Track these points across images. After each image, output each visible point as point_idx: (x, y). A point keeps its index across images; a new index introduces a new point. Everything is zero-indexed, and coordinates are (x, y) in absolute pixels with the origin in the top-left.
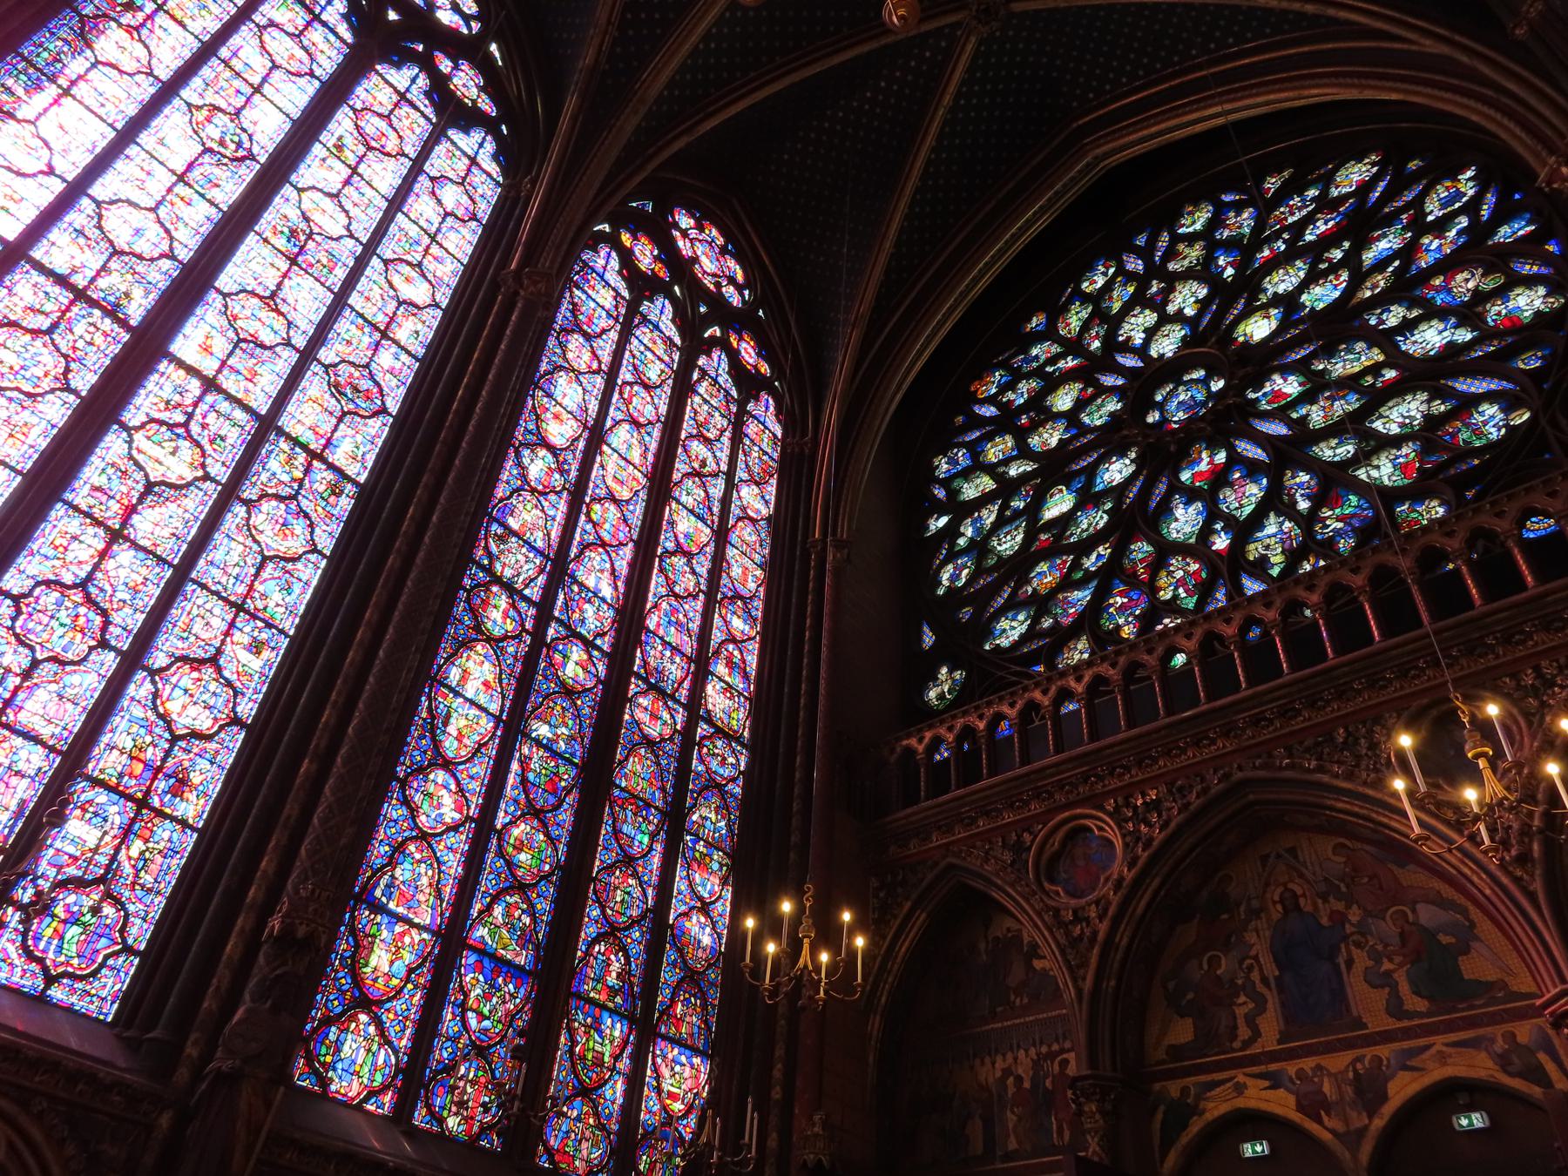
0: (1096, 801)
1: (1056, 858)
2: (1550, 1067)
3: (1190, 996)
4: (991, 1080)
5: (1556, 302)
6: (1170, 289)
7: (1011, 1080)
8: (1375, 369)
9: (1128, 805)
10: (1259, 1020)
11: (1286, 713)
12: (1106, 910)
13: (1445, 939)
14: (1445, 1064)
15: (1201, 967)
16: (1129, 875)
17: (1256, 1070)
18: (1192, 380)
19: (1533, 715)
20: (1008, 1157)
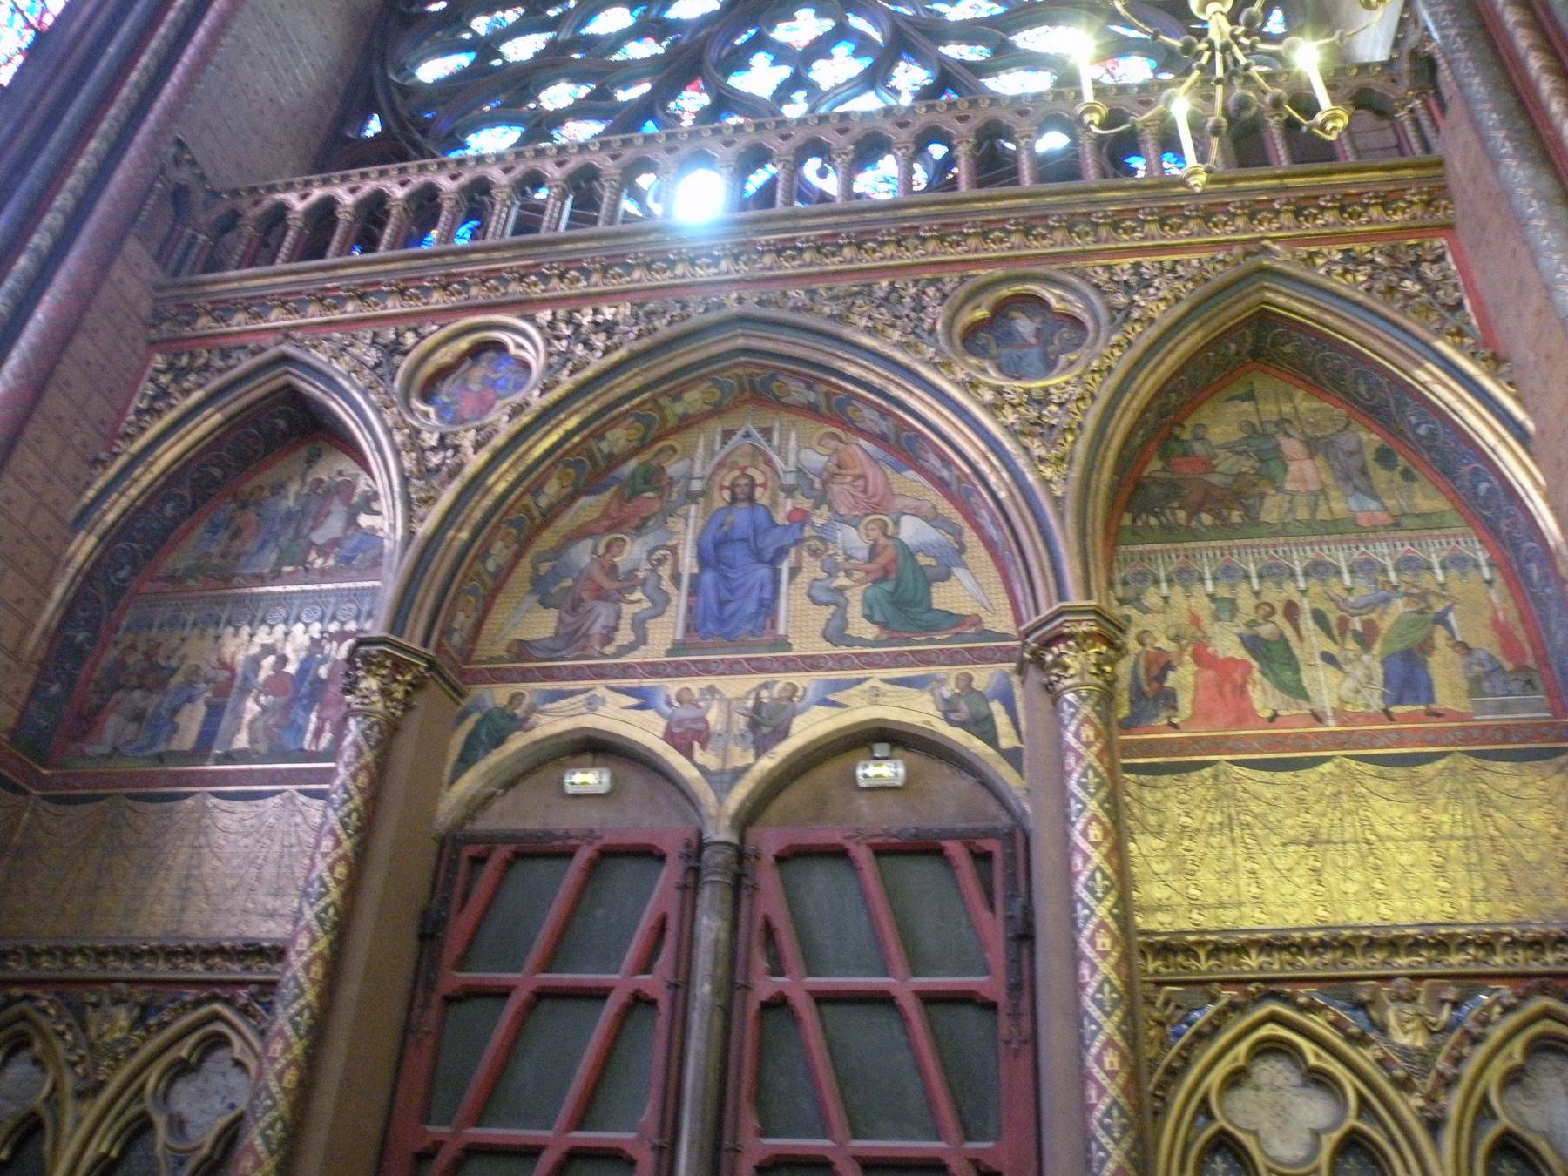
0: (524, 306)
1: (443, 373)
3: (567, 583)
4: (240, 657)
7: (269, 661)
9: (568, 322)
10: (650, 624)
12: (489, 437)
13: (923, 560)
14: (876, 703)
16: (537, 401)
20: (229, 757)
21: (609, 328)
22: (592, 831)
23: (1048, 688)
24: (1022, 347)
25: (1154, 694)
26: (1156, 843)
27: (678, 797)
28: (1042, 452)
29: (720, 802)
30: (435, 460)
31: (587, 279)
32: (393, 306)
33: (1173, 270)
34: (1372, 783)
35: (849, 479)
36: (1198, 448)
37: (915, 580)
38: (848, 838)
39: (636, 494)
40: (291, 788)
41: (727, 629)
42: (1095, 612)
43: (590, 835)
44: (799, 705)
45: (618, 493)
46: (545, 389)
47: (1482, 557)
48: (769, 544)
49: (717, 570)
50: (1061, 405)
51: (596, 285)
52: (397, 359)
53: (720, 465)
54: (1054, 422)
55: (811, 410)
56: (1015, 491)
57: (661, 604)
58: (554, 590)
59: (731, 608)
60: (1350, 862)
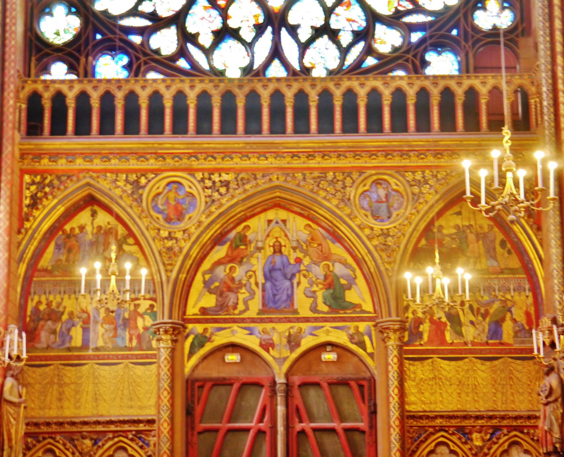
0: (191, 171)
1: (159, 194)
3: (217, 284)
4: (90, 309)
9: (210, 179)
10: (250, 302)
11: (310, 156)
13: (343, 281)
14: (328, 335)
15: (225, 271)
25: (416, 334)
26: (414, 383)
27: (263, 362)
29: (280, 369)
30: (169, 244)
32: (133, 164)
34: (479, 366)
39: (237, 247)
40: (126, 361)
41: (277, 306)
43: (237, 379)
44: (303, 335)
45: (231, 245)
47: (527, 286)
48: (289, 271)
49: (271, 282)
52: (141, 191)
53: (268, 236)
57: (252, 294)
58: (212, 287)
60: (469, 391)
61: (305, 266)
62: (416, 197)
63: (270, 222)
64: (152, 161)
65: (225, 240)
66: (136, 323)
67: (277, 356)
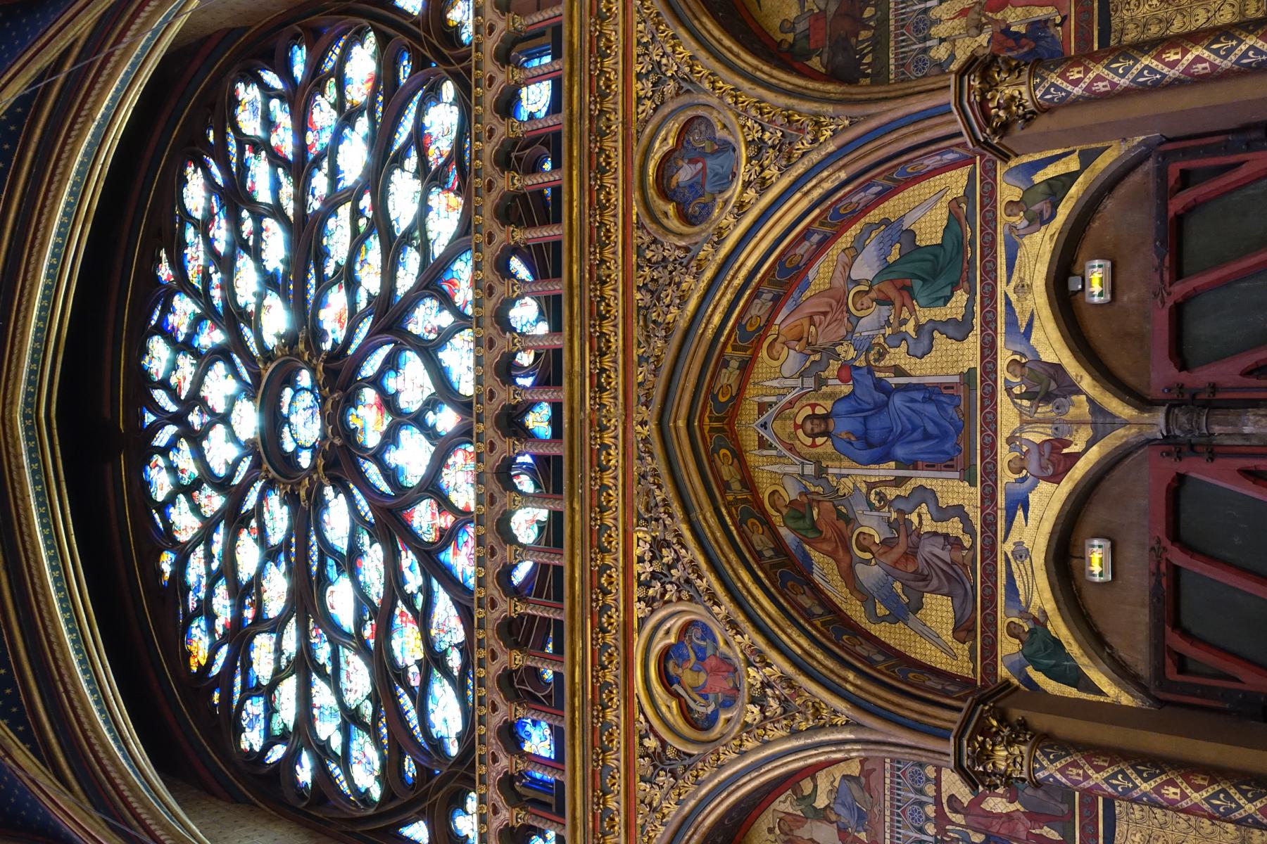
1: (685, 711)
2: (1051, 171)
3: (898, 586)
5: (371, 38)
6: (203, 402)
8: (356, 214)
9: (648, 585)
10: (943, 504)
12: (760, 652)
13: (894, 256)
14: (1030, 287)
15: (867, 562)
16: (726, 607)
17: (1001, 524)
18: (290, 405)
19: (680, 88)
21: (657, 546)
22: (1152, 549)
23: (1029, 118)
24: (705, 175)
27: (1117, 473)
28: (809, 137)
29: (1125, 424)
31: (610, 568)
32: (616, 760)
33: (646, 45)
35: (813, 329)
36: (801, 27)
37: (913, 261)
38: (1163, 303)
39: (814, 526)
42: (962, 77)
43: (1157, 551)
44: (1030, 357)
46: (713, 597)
48: (870, 396)
50: (763, 130)
51: (616, 560)
52: (670, 753)
53: (791, 448)
54: (779, 134)
55: (746, 367)
56: (841, 163)
57: (925, 495)
59: (931, 428)
61: (858, 356)
62: (686, 84)
63: (763, 444)
64: (610, 716)
65: (799, 556)
66: (1000, 815)
67: (1084, 435)
